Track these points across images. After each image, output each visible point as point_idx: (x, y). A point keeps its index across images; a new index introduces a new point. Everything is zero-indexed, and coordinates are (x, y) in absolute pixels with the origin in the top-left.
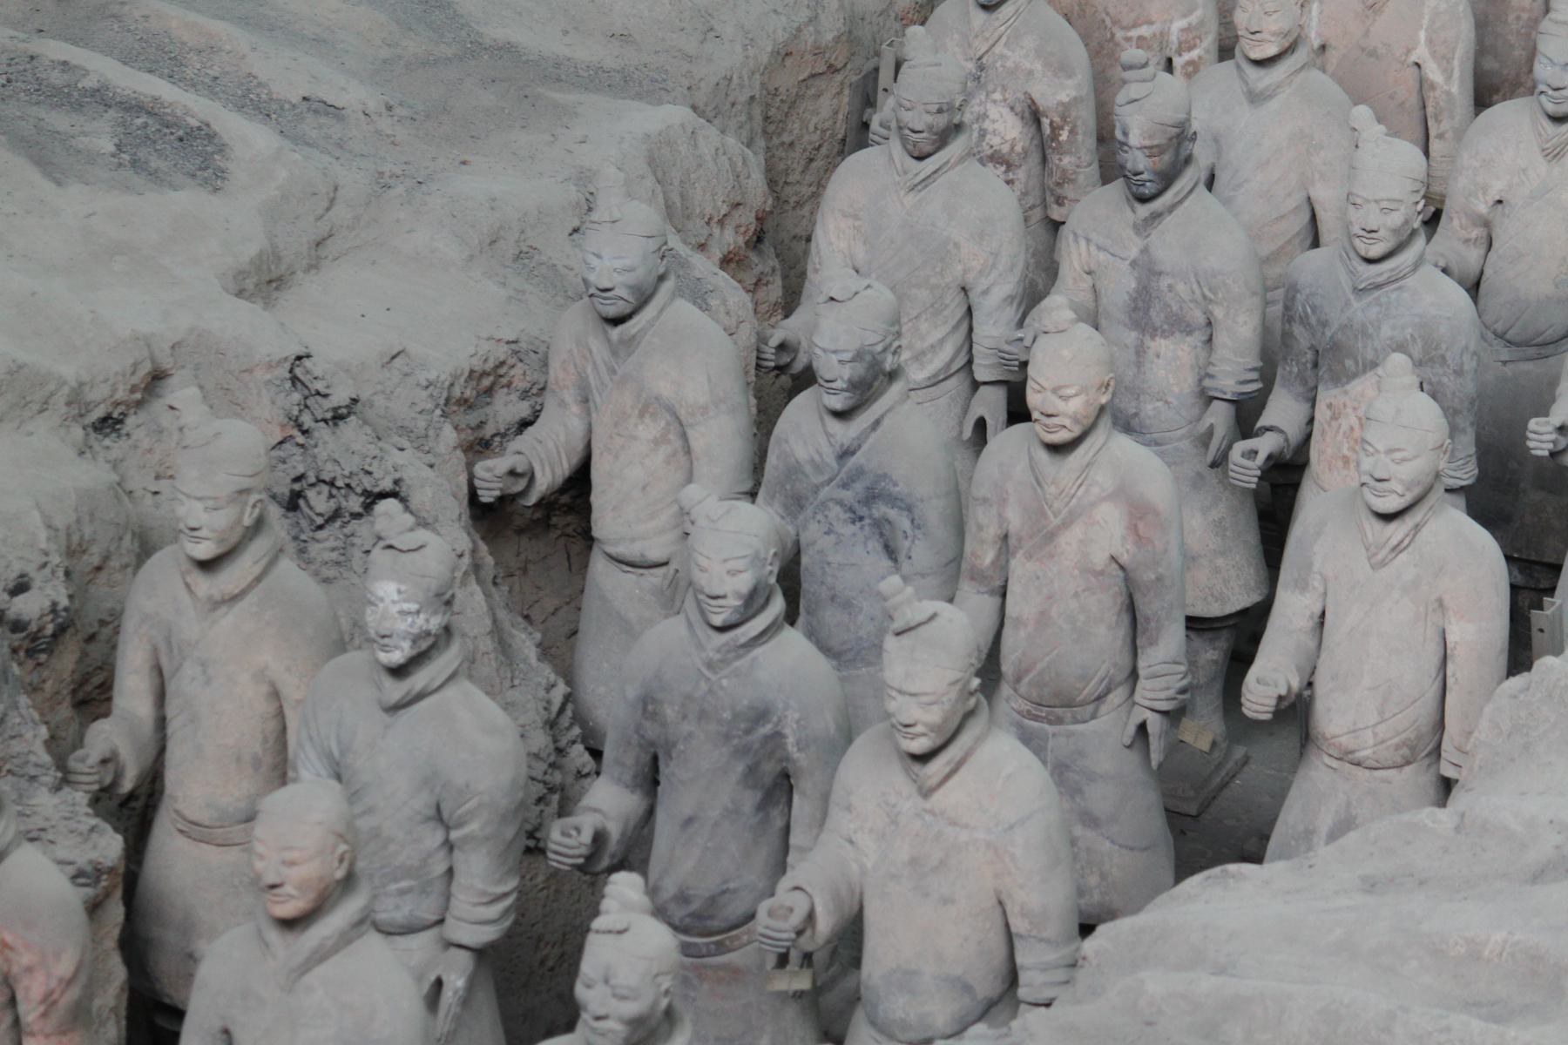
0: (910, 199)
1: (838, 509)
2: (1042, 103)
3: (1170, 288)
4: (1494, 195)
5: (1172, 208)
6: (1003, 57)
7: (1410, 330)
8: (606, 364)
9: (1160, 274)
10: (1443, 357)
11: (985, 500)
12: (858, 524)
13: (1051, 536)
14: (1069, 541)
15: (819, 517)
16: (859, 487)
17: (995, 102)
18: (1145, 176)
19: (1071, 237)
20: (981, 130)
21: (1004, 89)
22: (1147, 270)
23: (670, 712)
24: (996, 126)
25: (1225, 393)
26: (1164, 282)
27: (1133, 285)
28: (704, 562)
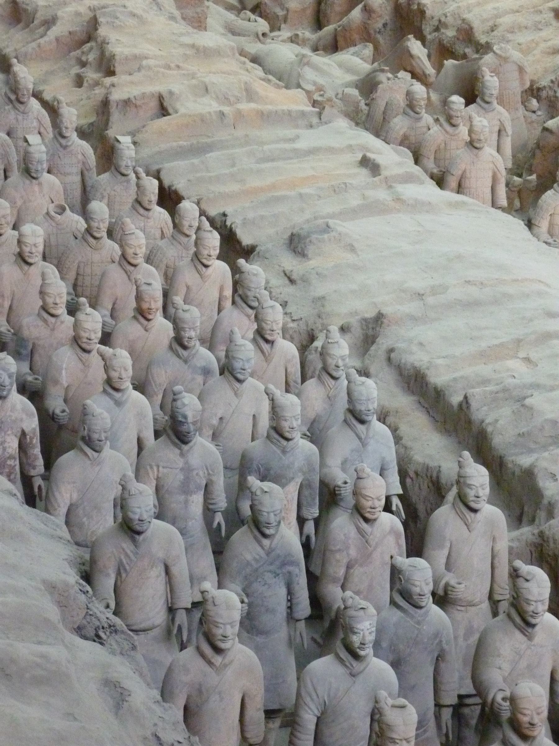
0: (97, 469)
1: (269, 574)
2: (27, 430)
3: (197, 474)
4: (219, 415)
5: (195, 444)
6: (10, 416)
7: (303, 462)
8: (132, 552)
9: (193, 470)
10: (314, 469)
11: (339, 550)
12: (277, 577)
13: (370, 555)
14: (376, 555)
15: (259, 580)
16: (277, 563)
17: (9, 435)
18: (193, 433)
19: (148, 467)
20: (3, 447)
21: (12, 428)
22: (187, 470)
23: (401, 647)
24: (10, 444)
25: (221, 508)
26: (195, 473)
27: (182, 477)
28: (417, 583)
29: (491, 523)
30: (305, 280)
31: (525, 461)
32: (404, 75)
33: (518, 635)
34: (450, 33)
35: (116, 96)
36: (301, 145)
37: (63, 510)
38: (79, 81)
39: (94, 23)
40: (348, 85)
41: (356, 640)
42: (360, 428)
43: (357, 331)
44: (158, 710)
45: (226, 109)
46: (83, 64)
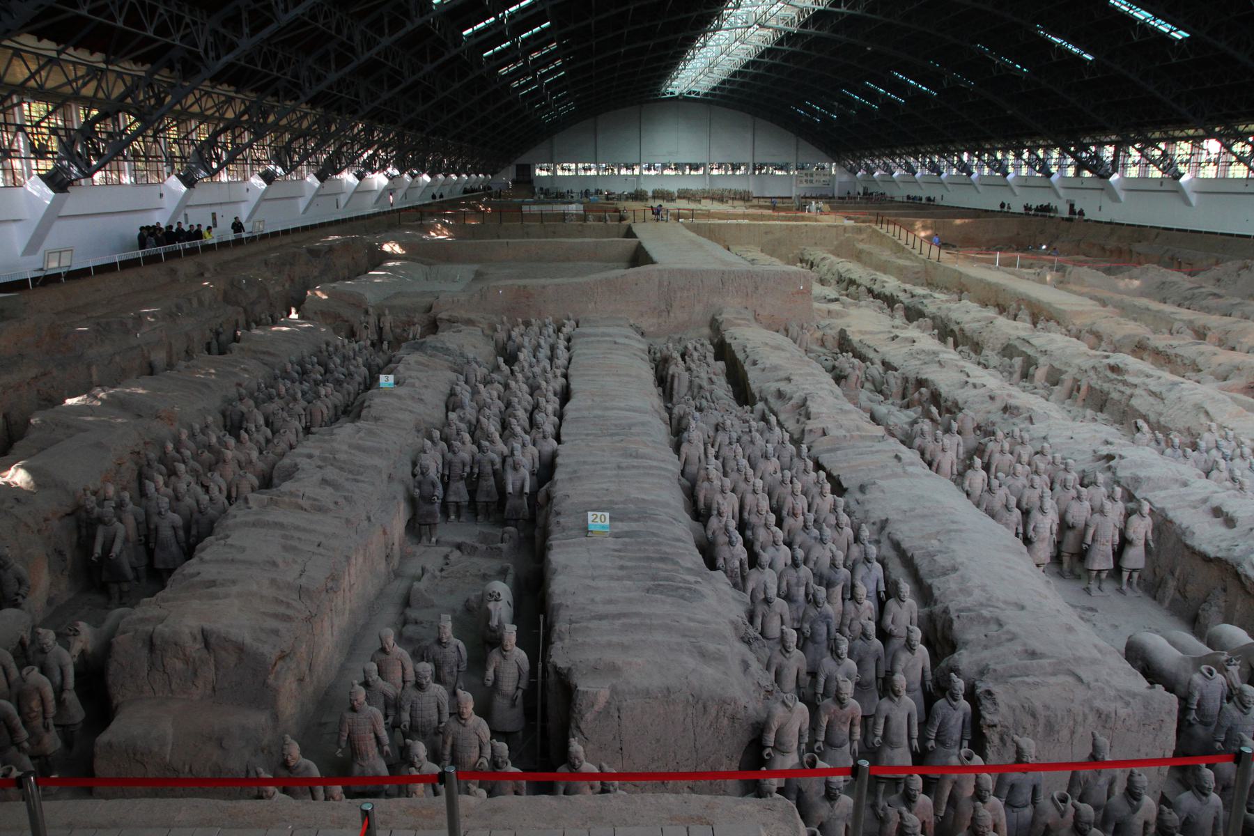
22: (798, 578)
29: (910, 606)
30: (863, 503)
31: (929, 581)
32: (927, 421)
33: (909, 653)
34: (949, 404)
35: (807, 428)
36: (873, 449)
37: (749, 591)
38: (798, 421)
39: (805, 400)
40: (906, 423)
41: (840, 652)
42: (869, 565)
43: (879, 525)
44: (761, 673)
45: (848, 434)
46: (800, 415)
